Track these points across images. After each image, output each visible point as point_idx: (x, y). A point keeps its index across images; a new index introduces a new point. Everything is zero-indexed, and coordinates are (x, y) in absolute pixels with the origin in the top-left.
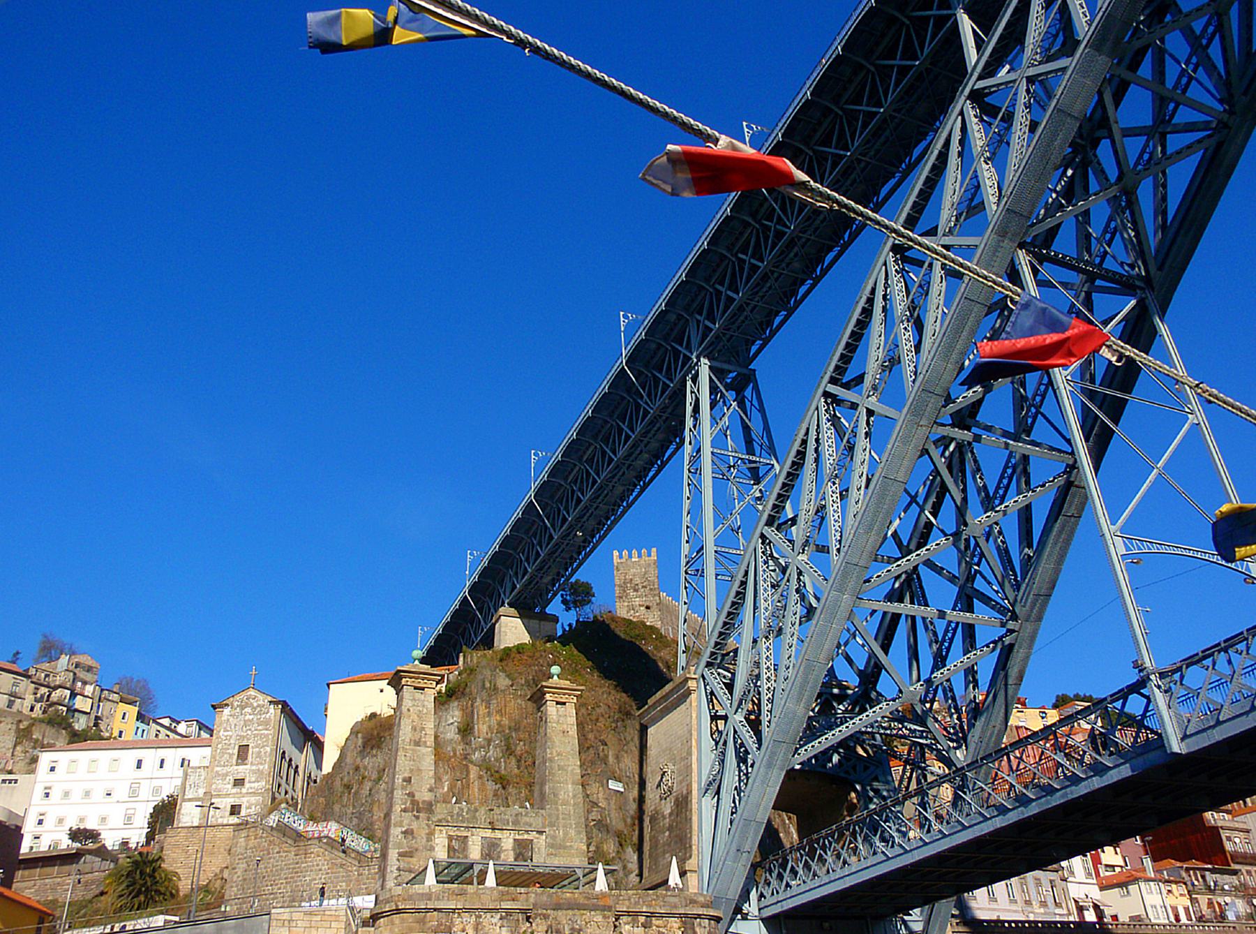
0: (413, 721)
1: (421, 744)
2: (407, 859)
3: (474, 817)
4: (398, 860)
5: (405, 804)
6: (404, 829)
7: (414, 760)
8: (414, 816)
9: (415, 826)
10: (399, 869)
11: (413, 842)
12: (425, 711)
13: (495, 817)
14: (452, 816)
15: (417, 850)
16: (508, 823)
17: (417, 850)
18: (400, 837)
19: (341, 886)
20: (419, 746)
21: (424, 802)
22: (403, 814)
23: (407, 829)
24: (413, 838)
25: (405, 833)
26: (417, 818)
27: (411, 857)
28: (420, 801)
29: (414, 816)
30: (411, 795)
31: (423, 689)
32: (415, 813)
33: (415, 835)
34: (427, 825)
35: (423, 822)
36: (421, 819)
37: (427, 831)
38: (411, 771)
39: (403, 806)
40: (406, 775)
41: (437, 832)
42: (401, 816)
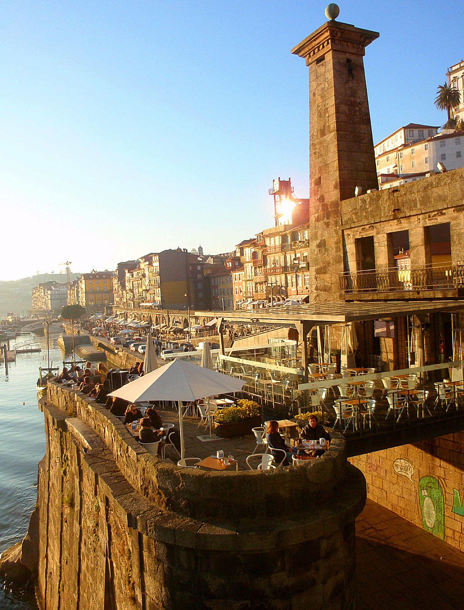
0: (318, 106)
2: (322, 276)
9: (326, 236)
10: (317, 289)
13: (400, 199)
16: (415, 206)
18: (316, 252)
22: (317, 223)
23: (321, 240)
25: (319, 246)
27: (325, 273)
32: (325, 220)
33: (327, 247)
35: (332, 228)
36: (330, 226)
39: (317, 215)
40: (317, 177)
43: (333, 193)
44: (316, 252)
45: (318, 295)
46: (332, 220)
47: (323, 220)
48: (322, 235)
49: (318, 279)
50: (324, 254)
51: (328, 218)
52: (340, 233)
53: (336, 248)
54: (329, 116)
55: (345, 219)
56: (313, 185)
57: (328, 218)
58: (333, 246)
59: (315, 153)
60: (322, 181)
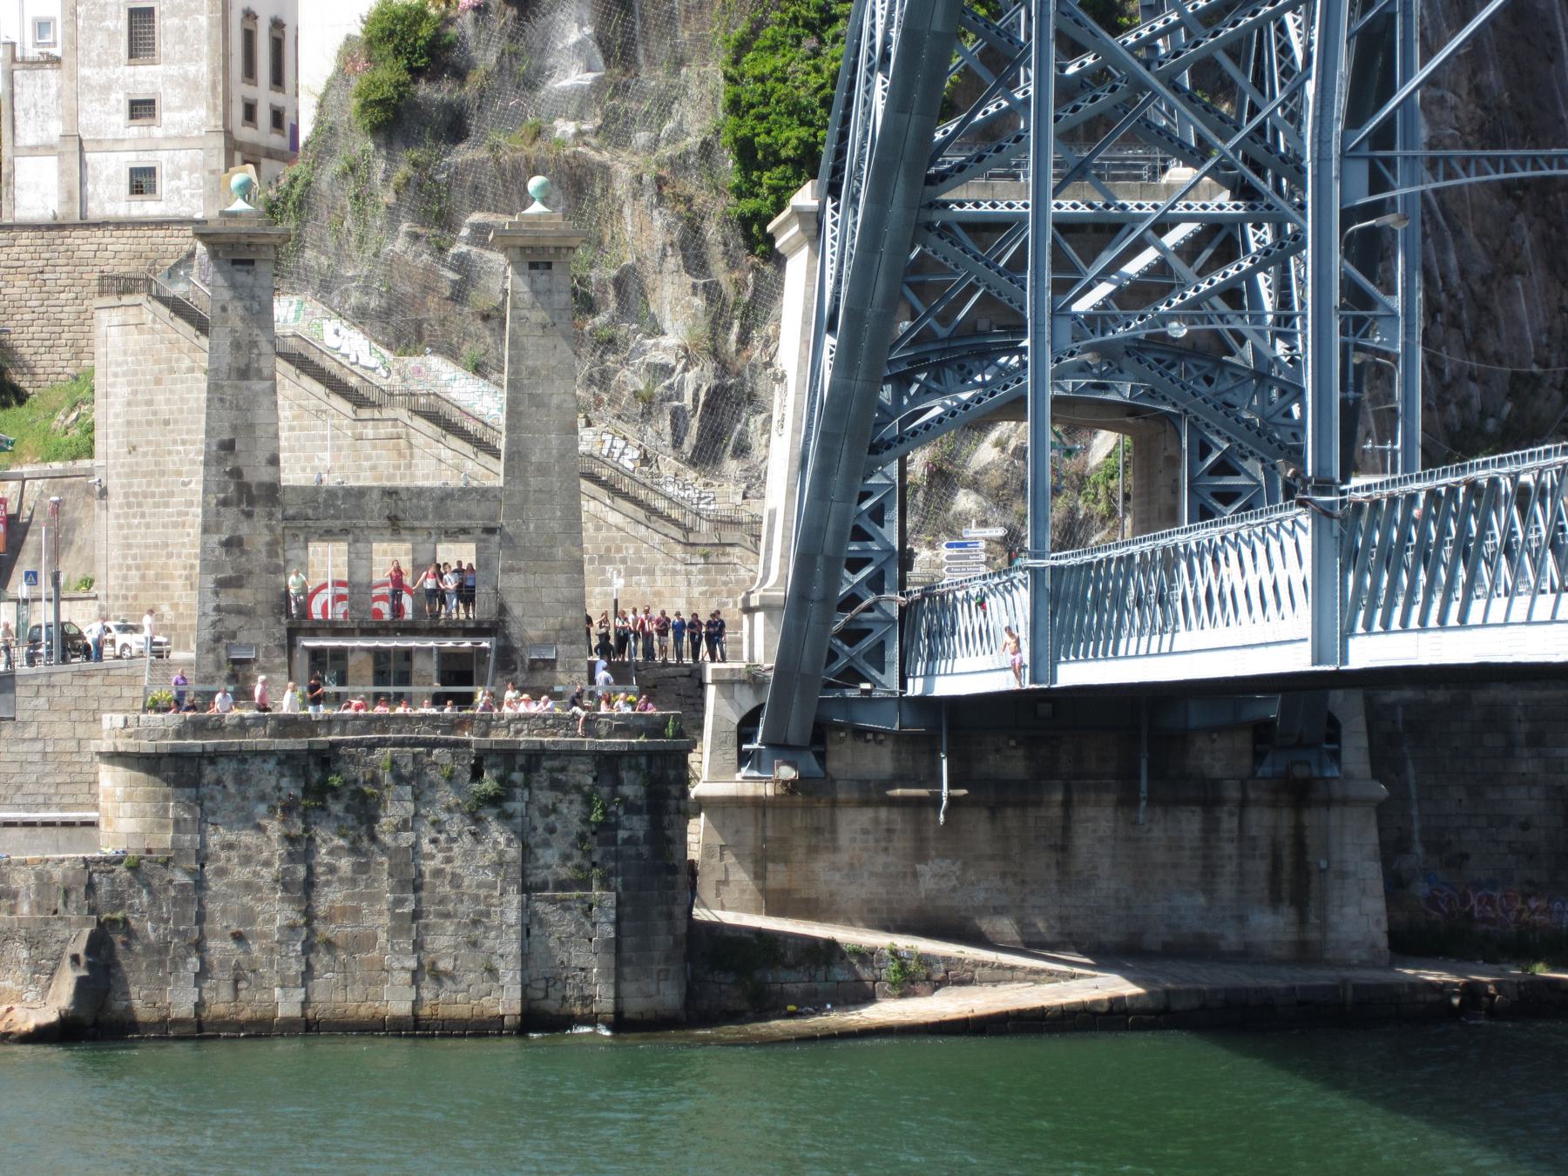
2: (232, 591)
3: (359, 507)
4: (216, 594)
5: (224, 490)
6: (224, 537)
7: (238, 408)
8: (243, 512)
9: (244, 530)
11: (243, 559)
14: (315, 509)
15: (250, 573)
17: (250, 573)
18: (217, 553)
19: (321, 459)
20: (248, 379)
21: (260, 485)
22: (222, 510)
24: (243, 552)
26: (249, 515)
27: (241, 586)
30: (236, 473)
32: (244, 506)
33: (247, 548)
35: (260, 520)
37: (268, 538)
38: (234, 428)
39: (222, 496)
41: (287, 538)
42: (218, 513)
44: (217, 553)
45: (220, 620)
46: (259, 510)
47: (238, 505)
48: (235, 529)
51: (251, 502)
54: (260, 354)
55: (291, 512)
56: (214, 448)
57: (251, 502)
58: (263, 549)
59: (222, 400)
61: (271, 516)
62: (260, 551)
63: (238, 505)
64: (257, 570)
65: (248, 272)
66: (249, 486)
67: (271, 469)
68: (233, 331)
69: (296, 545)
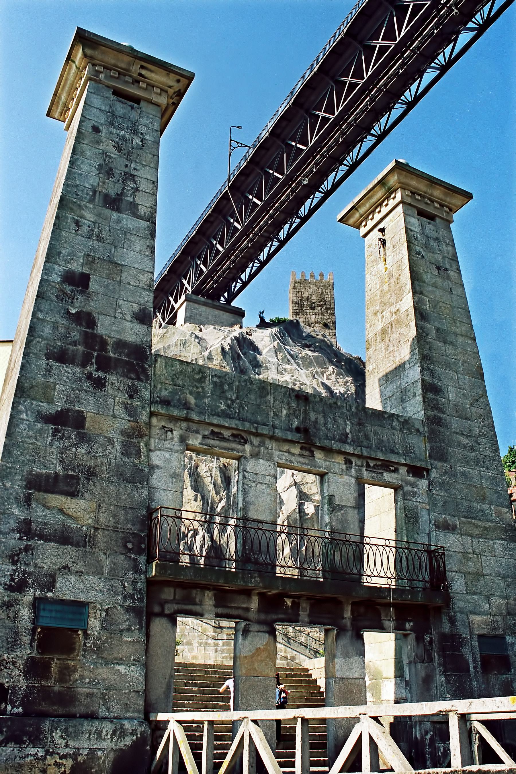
1: (123, 206)
8: (89, 377)
11: (81, 450)
12: (137, 141)
27: (72, 495)
28: (111, 342)
29: (89, 377)
31: (137, 100)
34: (126, 407)
37: (127, 425)
38: (90, 261)
41: (155, 431)
43: (128, 324)
47: (83, 365)
49: (34, 504)
50: (76, 445)
52: (144, 416)
53: (124, 445)
54: (137, 189)
58: (118, 439)
60: (93, 286)
61: (132, 393)
62: (111, 442)
63: (83, 365)
64: (105, 472)
65: (132, 108)
66: (103, 343)
67: (140, 328)
68: (105, 154)
69: (167, 444)
